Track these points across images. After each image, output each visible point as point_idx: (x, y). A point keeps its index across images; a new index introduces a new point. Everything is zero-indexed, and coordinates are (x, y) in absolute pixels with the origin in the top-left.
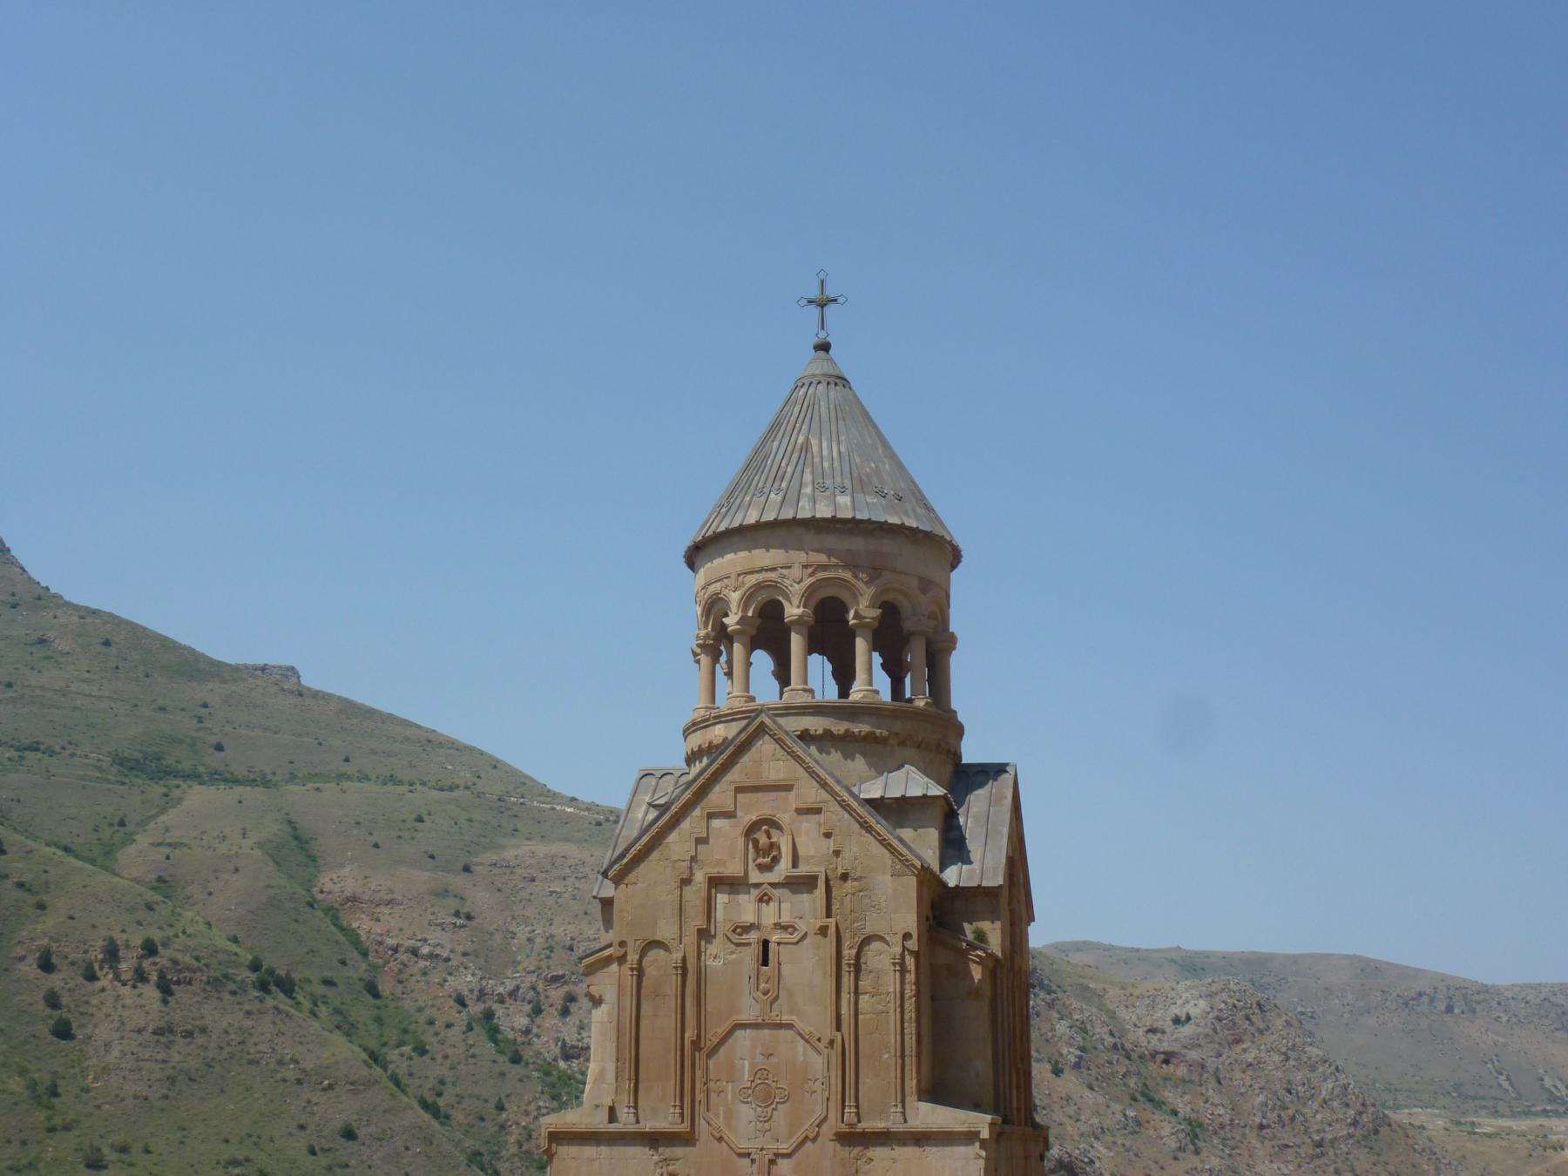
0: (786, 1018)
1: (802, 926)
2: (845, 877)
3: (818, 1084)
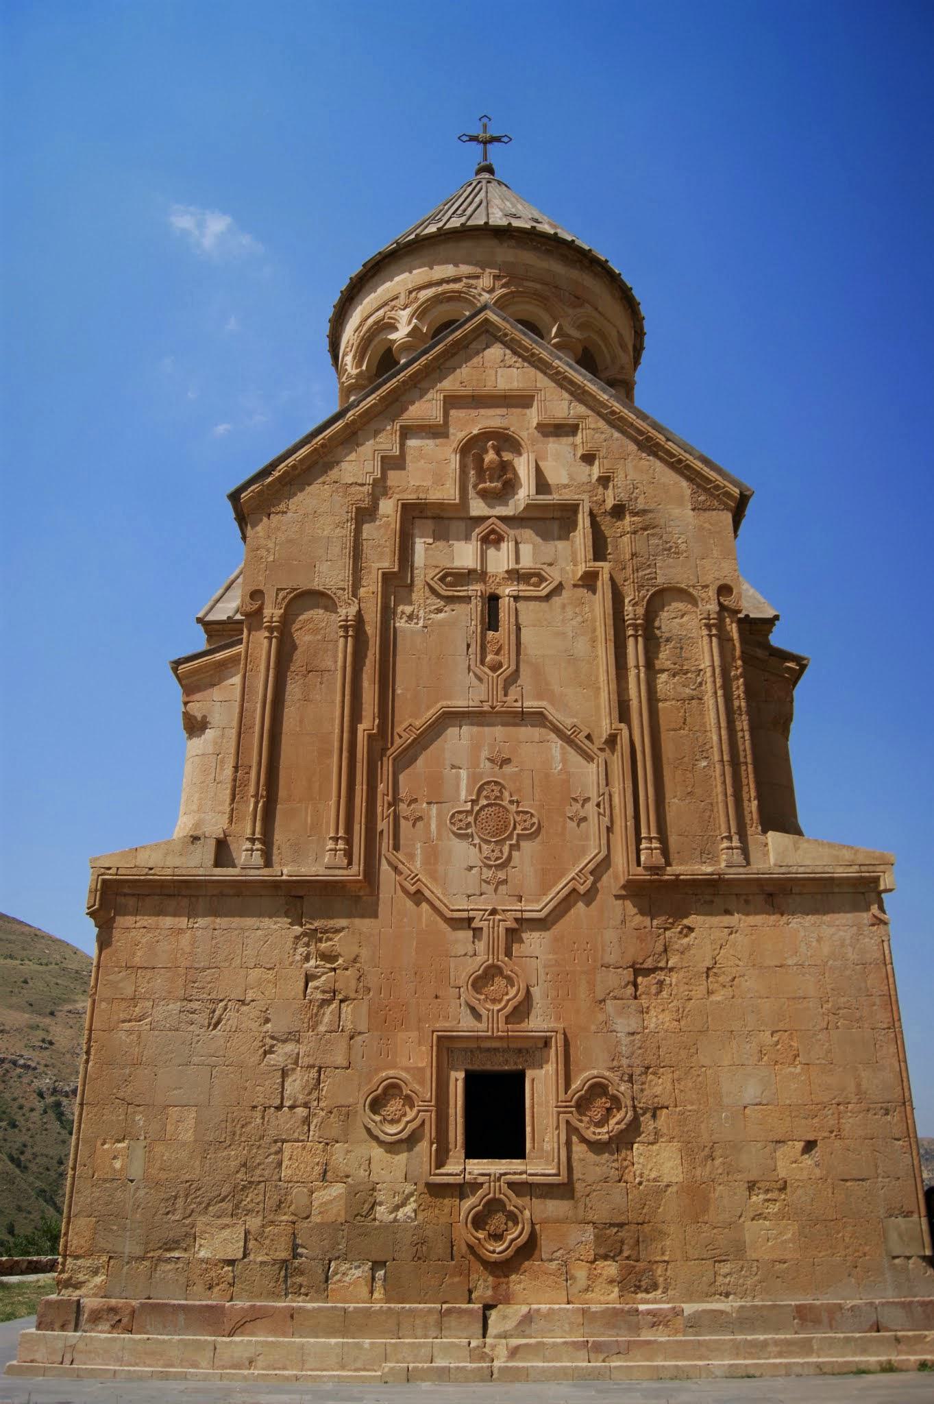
0: (530, 704)
1: (555, 575)
2: (618, 511)
3: (591, 808)
